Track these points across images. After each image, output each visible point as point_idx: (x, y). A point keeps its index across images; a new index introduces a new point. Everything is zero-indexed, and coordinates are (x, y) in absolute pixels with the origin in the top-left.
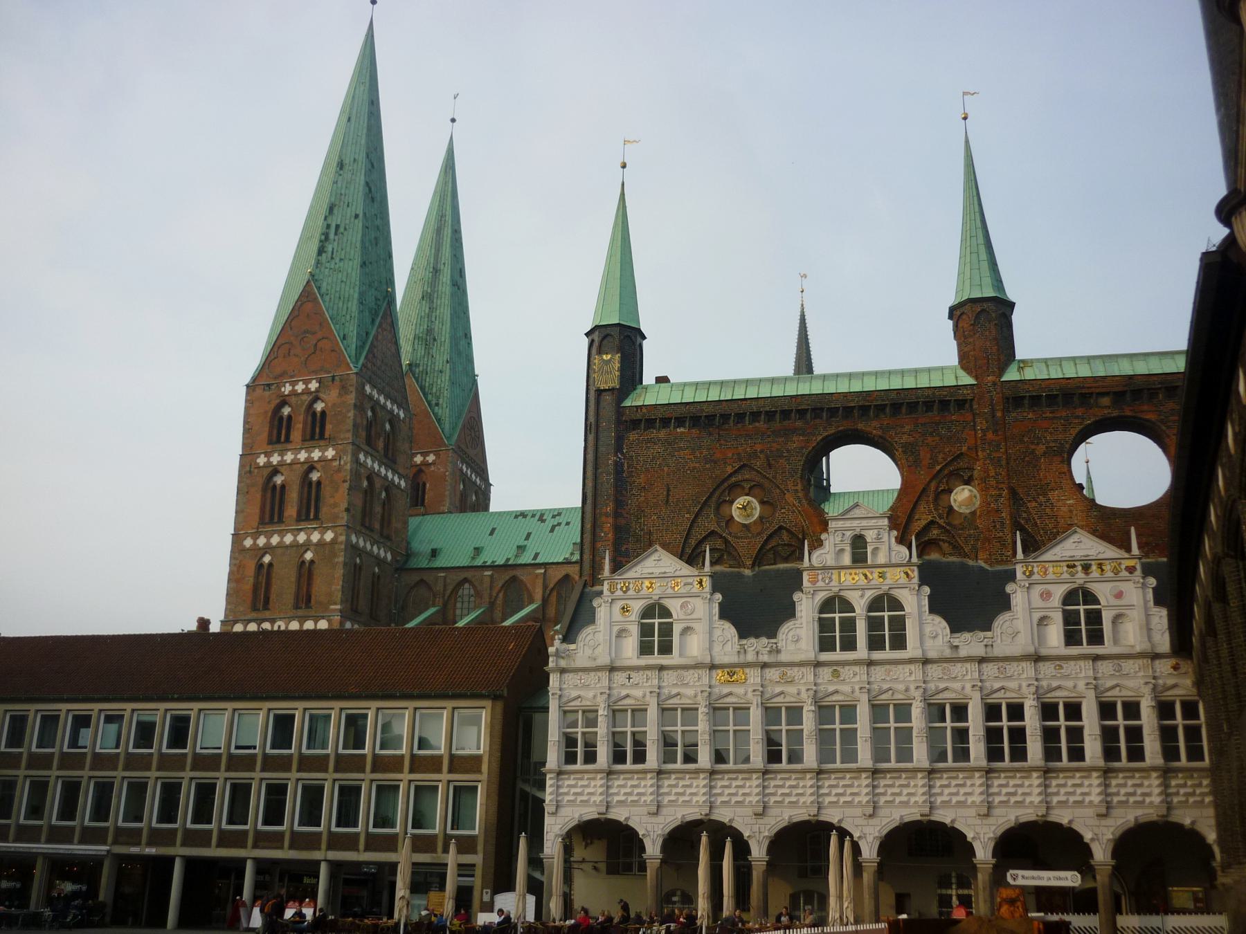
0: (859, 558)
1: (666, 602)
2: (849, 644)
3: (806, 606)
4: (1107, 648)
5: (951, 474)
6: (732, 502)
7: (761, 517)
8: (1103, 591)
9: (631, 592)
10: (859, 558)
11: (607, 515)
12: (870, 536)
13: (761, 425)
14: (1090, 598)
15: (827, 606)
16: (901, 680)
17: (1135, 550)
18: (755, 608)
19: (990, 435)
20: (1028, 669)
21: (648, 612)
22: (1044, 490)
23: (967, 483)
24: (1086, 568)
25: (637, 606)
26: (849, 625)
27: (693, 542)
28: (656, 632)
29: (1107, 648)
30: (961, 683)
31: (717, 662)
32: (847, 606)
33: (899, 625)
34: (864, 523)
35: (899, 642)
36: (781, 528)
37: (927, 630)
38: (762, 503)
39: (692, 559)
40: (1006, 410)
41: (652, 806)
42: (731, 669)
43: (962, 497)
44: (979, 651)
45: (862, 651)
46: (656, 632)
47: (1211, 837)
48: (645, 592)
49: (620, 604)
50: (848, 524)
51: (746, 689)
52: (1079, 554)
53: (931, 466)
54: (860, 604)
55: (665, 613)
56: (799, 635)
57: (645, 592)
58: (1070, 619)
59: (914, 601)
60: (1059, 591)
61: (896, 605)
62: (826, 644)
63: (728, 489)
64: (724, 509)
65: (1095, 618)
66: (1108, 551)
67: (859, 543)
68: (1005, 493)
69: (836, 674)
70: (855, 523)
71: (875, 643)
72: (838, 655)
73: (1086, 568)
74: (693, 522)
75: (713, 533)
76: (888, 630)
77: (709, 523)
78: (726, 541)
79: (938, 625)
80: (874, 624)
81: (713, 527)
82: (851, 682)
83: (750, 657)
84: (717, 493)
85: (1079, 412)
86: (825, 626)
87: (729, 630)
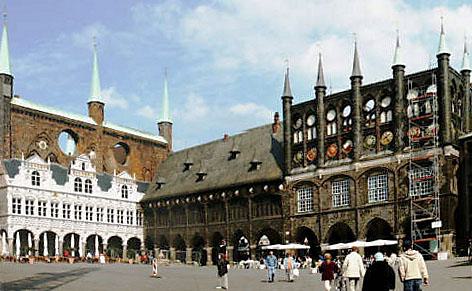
2: (80, 190)
3: (72, 178)
4: (128, 199)
8: (129, 187)
12: (86, 164)
13: (48, 121)
16: (83, 201)
18: (61, 177)
20: (115, 202)
21: (34, 173)
22: (109, 157)
25: (31, 171)
26: (81, 185)
29: (128, 199)
30: (105, 204)
32: (80, 180)
33: (91, 187)
35: (91, 192)
39: (46, 160)
41: (37, 227)
42: (56, 193)
43: (92, 153)
45: (83, 192)
47: (142, 240)
51: (60, 199)
54: (83, 180)
55: (38, 174)
56: (70, 186)
59: (95, 182)
66: (130, 178)
71: (86, 191)
72: (78, 193)
76: (89, 189)
79: (99, 189)
80: (86, 186)
81: (35, 148)
82: (83, 201)
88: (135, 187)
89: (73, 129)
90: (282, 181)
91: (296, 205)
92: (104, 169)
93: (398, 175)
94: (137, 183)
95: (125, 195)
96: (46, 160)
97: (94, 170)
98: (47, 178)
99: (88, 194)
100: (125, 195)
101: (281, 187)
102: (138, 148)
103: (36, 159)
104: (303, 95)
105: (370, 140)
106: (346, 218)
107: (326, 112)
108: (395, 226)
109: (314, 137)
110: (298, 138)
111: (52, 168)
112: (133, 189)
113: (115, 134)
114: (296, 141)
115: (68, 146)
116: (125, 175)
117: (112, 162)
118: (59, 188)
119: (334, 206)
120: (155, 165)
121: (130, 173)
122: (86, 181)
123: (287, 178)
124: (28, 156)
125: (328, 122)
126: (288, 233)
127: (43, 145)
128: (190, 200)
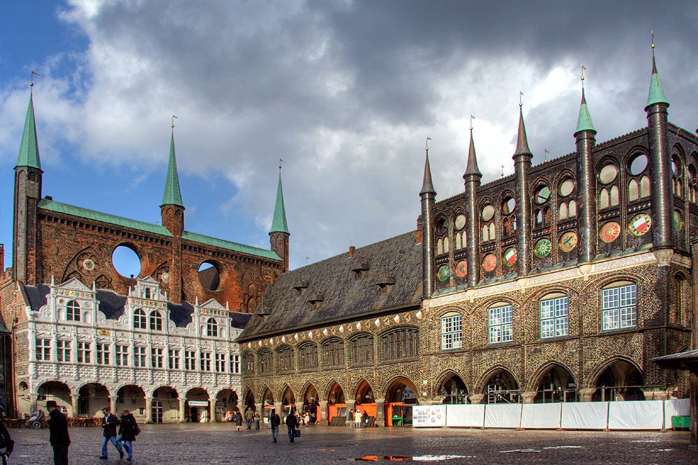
0: (148, 296)
1: (78, 301)
2: (144, 326)
3: (129, 311)
5: (163, 267)
6: (83, 260)
7: (95, 269)
8: (218, 320)
9: (64, 295)
10: (148, 296)
11: (32, 255)
14: (215, 322)
15: (137, 312)
17: (228, 309)
19: (176, 257)
21: (70, 303)
22: (191, 280)
23: (167, 272)
24: (215, 312)
26: (144, 320)
27: (67, 274)
28: (74, 312)
29: (218, 337)
31: (99, 327)
32: (143, 313)
33: (159, 321)
34: (151, 284)
36: (103, 275)
37: (168, 325)
38: (95, 263)
40: (182, 249)
43: (165, 276)
44: (184, 334)
46: (74, 312)
48: (70, 295)
49: (60, 298)
50: (146, 283)
52: (214, 307)
53: (157, 264)
55: (77, 305)
57: (70, 295)
58: (209, 327)
59: (165, 314)
60: (208, 318)
61: (159, 315)
62: (136, 325)
63: (81, 255)
64: (80, 262)
65: (215, 328)
66: (222, 308)
67: (148, 290)
68: (180, 279)
69: (140, 336)
70: (148, 284)
71: (152, 327)
73: (215, 312)
74: (68, 265)
75: (75, 271)
76: (156, 324)
77: (74, 267)
78: (81, 276)
79: (172, 323)
80: (152, 320)
81: (76, 269)
83: (111, 327)
84: (78, 255)
85: (203, 255)
86: (136, 318)
87: (103, 316)
88: (227, 321)
89: (134, 239)
90: (418, 307)
91: (440, 340)
92: (184, 297)
93: (578, 296)
94: (231, 315)
95: (213, 331)
96: (91, 288)
97: (164, 298)
98: (92, 314)
99: (155, 331)
100: (213, 331)
101: (419, 314)
102: (236, 268)
103: (75, 285)
104: (450, 185)
105: (544, 247)
106: (508, 360)
107: (480, 208)
108: (580, 375)
109: (465, 245)
110: (444, 246)
111: (99, 296)
112: (224, 323)
113: (200, 249)
114: (440, 252)
115: (126, 262)
116: (214, 304)
117: (196, 287)
118: (111, 323)
119: (494, 338)
120: (263, 290)
121: (222, 302)
122: (153, 314)
123: (425, 302)
124: (64, 279)
125: (483, 222)
126: (425, 382)
127: (89, 264)
128: (299, 337)
